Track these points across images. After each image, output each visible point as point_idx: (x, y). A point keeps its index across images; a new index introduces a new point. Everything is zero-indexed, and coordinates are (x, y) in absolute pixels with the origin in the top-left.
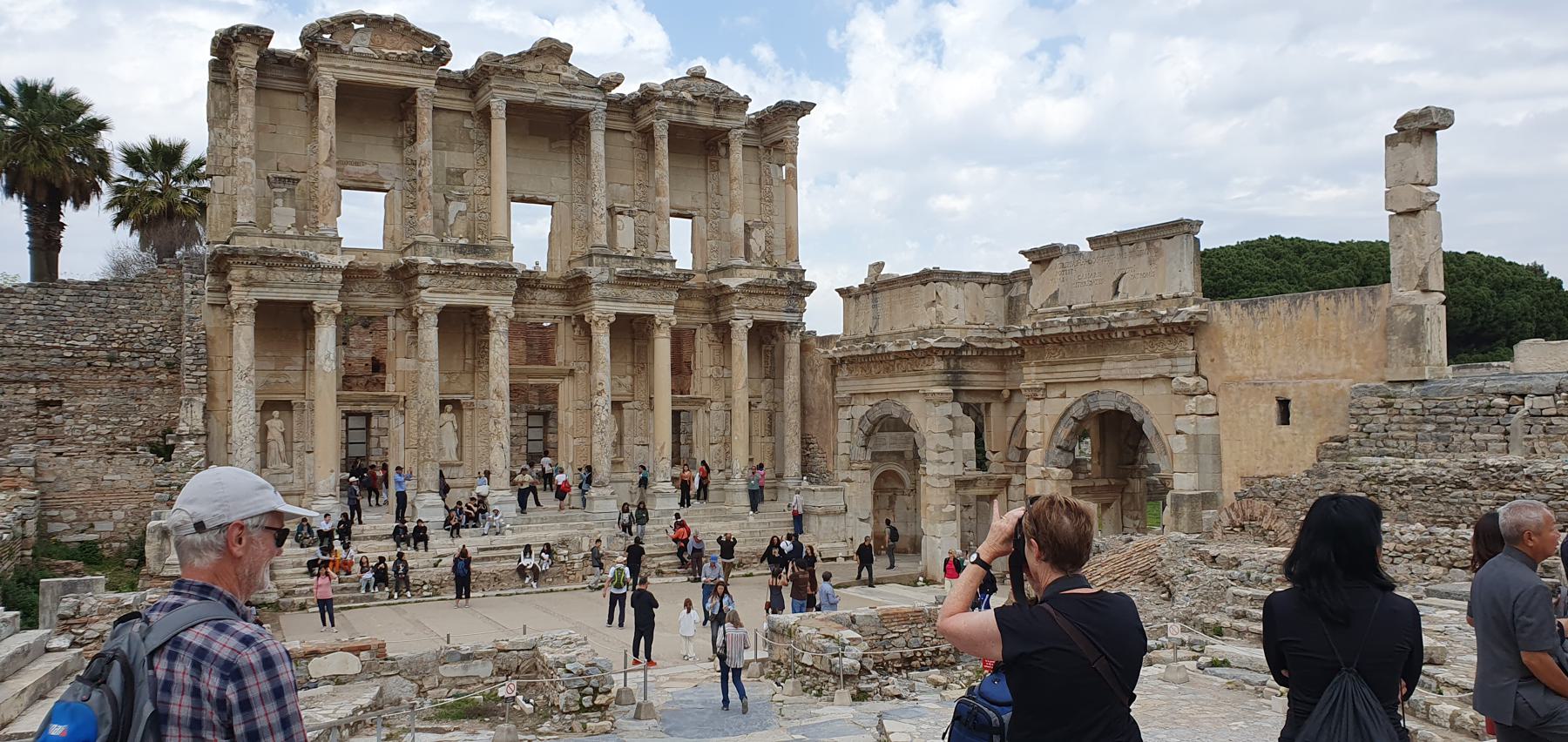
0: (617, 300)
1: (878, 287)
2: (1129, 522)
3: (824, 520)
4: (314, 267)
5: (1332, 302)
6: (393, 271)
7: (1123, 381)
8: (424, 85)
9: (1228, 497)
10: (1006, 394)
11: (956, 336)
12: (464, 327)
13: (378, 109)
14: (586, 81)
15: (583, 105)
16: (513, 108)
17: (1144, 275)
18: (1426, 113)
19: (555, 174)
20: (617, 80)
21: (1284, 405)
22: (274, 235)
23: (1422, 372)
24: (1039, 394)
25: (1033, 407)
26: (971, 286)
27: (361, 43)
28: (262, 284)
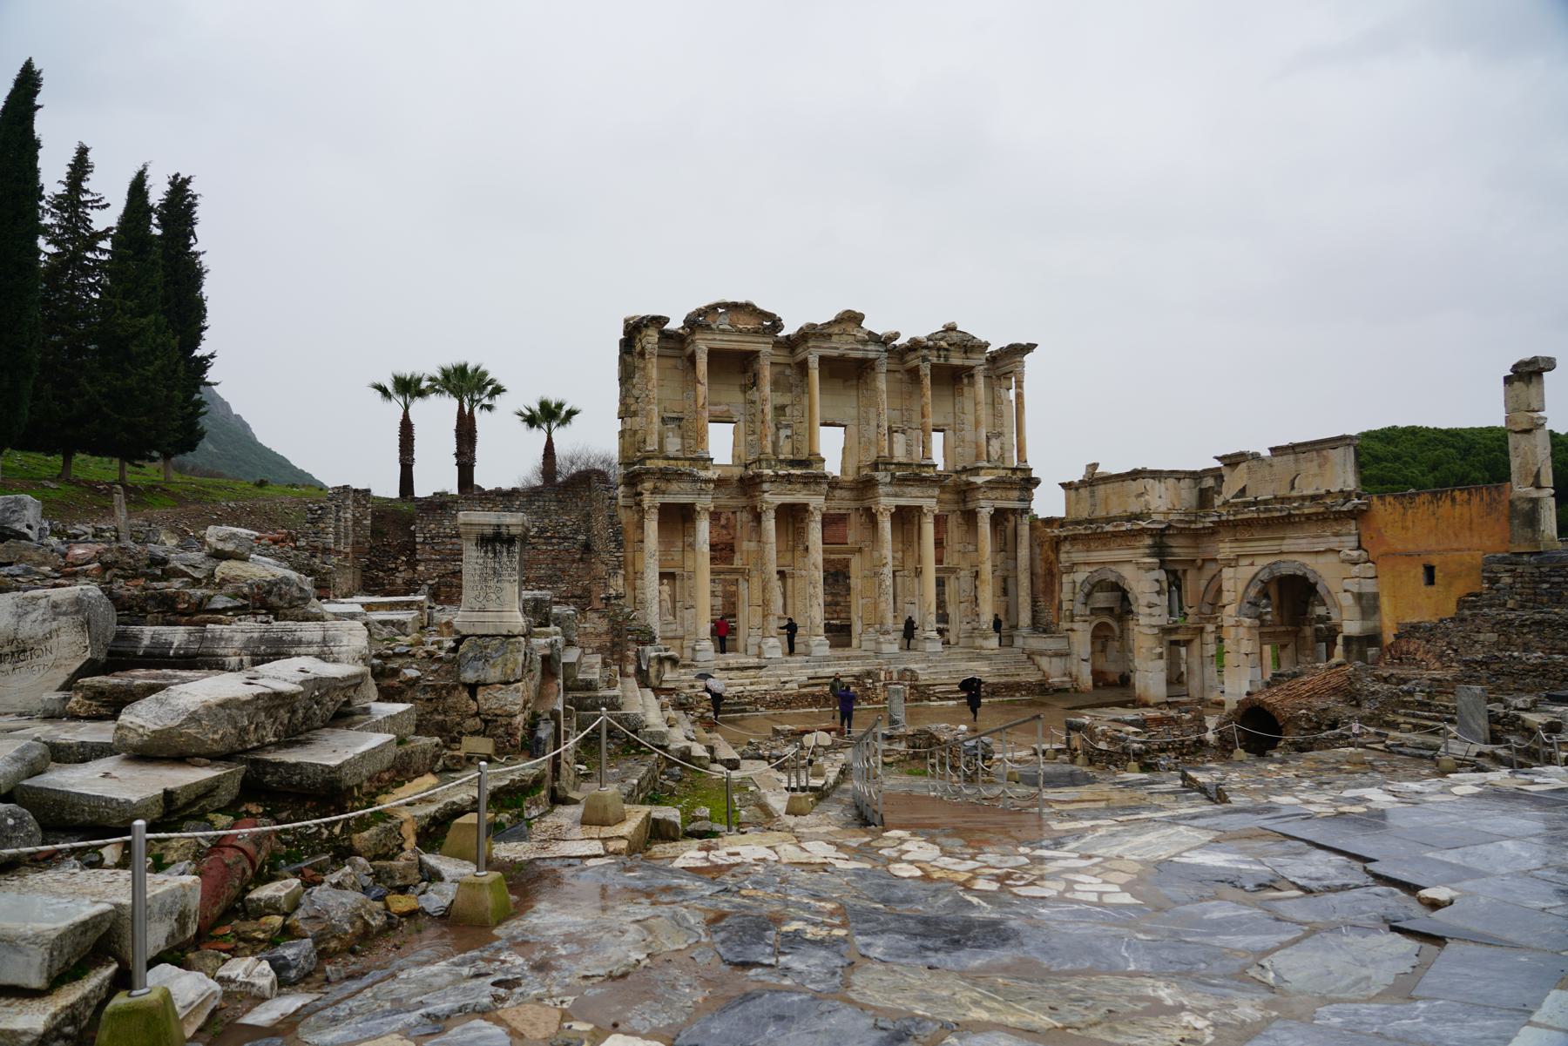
0: (896, 495)
1: (1093, 480)
2: (1302, 659)
3: (1055, 660)
4: (695, 479)
5: (1465, 495)
6: (741, 479)
7: (1303, 553)
8: (764, 347)
9: (1388, 638)
10: (1199, 562)
11: (1158, 521)
12: (792, 517)
13: (734, 366)
14: (874, 338)
15: (872, 355)
16: (823, 360)
17: (1315, 475)
18: (1535, 360)
19: (847, 405)
20: (896, 335)
21: (1430, 572)
22: (668, 458)
23: (1538, 546)
24: (1232, 563)
25: (1227, 573)
26: (1171, 482)
27: (723, 322)
28: (664, 493)
